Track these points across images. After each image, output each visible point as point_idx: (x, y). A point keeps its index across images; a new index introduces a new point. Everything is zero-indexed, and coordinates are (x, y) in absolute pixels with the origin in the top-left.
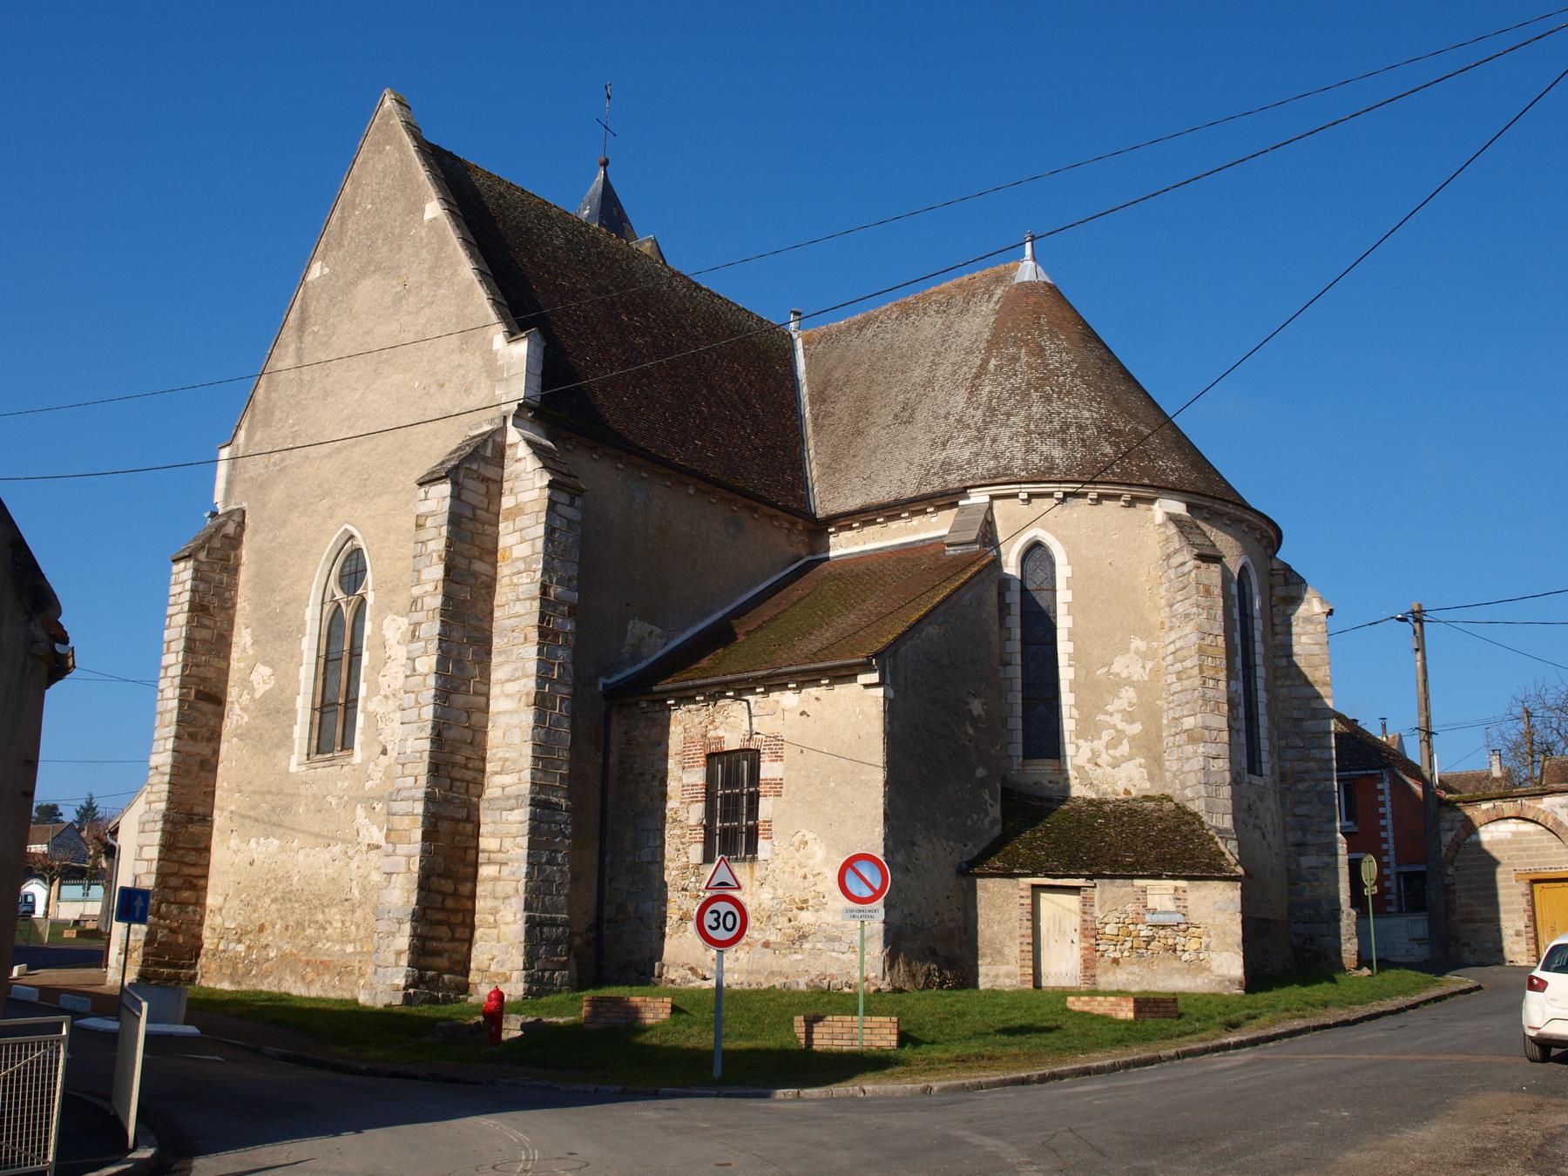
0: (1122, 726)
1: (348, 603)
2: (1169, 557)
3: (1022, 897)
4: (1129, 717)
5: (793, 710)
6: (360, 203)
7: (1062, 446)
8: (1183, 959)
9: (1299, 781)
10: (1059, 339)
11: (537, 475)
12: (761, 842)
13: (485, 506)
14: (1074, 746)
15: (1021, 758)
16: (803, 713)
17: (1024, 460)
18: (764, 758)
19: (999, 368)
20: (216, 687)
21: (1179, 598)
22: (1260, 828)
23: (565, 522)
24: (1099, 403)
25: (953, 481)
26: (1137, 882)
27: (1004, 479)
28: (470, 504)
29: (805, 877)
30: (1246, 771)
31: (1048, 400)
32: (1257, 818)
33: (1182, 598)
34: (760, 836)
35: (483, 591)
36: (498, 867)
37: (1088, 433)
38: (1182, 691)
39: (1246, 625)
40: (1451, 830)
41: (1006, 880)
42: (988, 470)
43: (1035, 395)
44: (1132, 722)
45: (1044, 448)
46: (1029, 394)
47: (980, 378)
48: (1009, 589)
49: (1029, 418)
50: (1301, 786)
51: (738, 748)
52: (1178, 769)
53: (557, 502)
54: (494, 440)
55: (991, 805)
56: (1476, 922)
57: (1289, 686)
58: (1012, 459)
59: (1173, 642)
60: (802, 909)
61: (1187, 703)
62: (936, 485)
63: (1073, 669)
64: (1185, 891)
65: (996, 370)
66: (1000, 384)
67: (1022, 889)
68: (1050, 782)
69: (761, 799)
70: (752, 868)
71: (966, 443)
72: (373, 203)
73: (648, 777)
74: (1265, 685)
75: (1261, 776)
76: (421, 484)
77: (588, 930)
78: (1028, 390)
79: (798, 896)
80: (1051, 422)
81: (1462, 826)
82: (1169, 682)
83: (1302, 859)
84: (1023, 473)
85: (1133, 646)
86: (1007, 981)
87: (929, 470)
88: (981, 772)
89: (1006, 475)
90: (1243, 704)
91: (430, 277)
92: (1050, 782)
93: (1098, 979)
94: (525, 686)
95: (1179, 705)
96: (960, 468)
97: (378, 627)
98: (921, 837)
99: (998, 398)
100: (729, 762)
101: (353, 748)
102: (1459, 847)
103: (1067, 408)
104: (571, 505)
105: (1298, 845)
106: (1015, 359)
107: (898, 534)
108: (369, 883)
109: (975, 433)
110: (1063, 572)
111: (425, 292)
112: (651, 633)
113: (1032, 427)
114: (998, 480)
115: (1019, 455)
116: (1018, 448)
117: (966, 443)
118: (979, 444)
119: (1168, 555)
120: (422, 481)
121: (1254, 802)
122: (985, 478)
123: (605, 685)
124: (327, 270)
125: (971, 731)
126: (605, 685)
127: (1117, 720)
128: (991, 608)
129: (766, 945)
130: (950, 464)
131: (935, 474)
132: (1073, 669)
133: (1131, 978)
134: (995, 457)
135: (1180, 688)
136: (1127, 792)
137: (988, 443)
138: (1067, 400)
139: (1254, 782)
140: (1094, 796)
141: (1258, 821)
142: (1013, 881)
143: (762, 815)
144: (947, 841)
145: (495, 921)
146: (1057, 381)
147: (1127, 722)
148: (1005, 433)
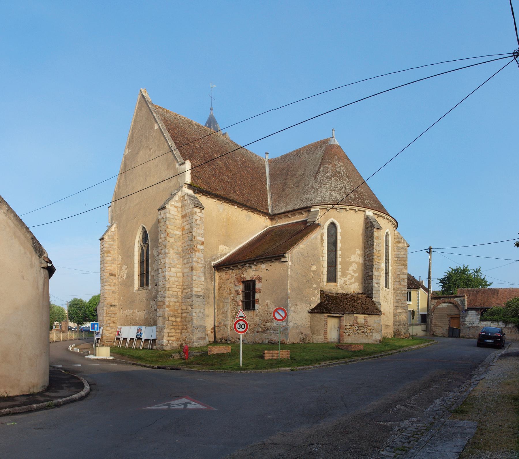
0: (353, 274)
1: (144, 246)
2: (368, 228)
3: (325, 319)
4: (354, 272)
5: (264, 269)
6: (137, 128)
7: (340, 194)
8: (366, 335)
9: (398, 290)
10: (340, 162)
11: (191, 204)
12: (256, 305)
13: (177, 215)
14: (340, 279)
15: (326, 282)
16: (267, 270)
17: (329, 198)
18: (256, 282)
19: (323, 170)
20: (114, 272)
21: (370, 240)
22: (387, 302)
23: (199, 217)
24: (351, 182)
25: (309, 204)
26: (355, 315)
27: (323, 204)
28: (173, 214)
29: (268, 314)
30: (385, 287)
31: (337, 181)
32: (387, 299)
33: (370, 240)
34: (256, 303)
35: (178, 239)
36: (186, 314)
37: (347, 191)
38: (369, 265)
39: (387, 248)
40: (433, 304)
41: (320, 314)
42: (319, 201)
43: (333, 179)
44: (356, 273)
45: (335, 195)
46: (331, 179)
47: (318, 173)
48: (324, 235)
49: (331, 186)
50: (398, 292)
51: (249, 280)
52: (367, 286)
53: (197, 212)
54: (178, 195)
55: (318, 295)
56: (437, 327)
57: (397, 266)
58: (326, 198)
59: (368, 252)
60: (267, 322)
61: (370, 268)
62: (304, 205)
63: (341, 258)
64: (367, 318)
65: (322, 171)
66: (323, 175)
67: (325, 317)
68: (334, 289)
69: (256, 294)
70: (254, 312)
71: (313, 193)
72: (140, 127)
73: (226, 288)
74: (391, 265)
75: (388, 288)
76: (159, 210)
77: (212, 329)
78: (331, 177)
79: (266, 319)
80: (337, 187)
81: (436, 304)
82: (366, 263)
83: (397, 310)
84: (329, 202)
85: (356, 252)
86: (321, 340)
87: (303, 201)
88: (315, 286)
89: (324, 202)
90: (385, 269)
91: (158, 148)
92: (334, 289)
93: (344, 339)
94: (191, 265)
95: (368, 269)
96: (311, 200)
97: (152, 252)
98: (299, 303)
99: (323, 180)
100: (247, 284)
101: (148, 285)
102: (435, 308)
103: (342, 183)
104: (201, 212)
105: (397, 307)
106: (328, 168)
107: (294, 219)
108: (155, 319)
109: (316, 190)
110: (339, 231)
111: (157, 153)
112: (226, 249)
113: (332, 188)
114: (322, 204)
115: (328, 197)
116: (327, 194)
117: (313, 193)
118: (317, 193)
119: (367, 227)
120: (159, 209)
121: (386, 295)
122: (318, 203)
123: (213, 264)
124: (130, 150)
125: (312, 275)
126: (213, 264)
127: (351, 272)
128: (319, 241)
129: (258, 332)
130: (308, 199)
131: (304, 202)
132: (341, 258)
133: (352, 339)
134: (321, 197)
135: (368, 265)
136: (354, 292)
137: (319, 193)
138: (342, 181)
139: (386, 290)
140: (345, 293)
141: (387, 300)
142: (323, 315)
143: (256, 298)
144: (305, 304)
145: (186, 328)
146: (339, 175)
147: (354, 273)
148: (324, 190)
